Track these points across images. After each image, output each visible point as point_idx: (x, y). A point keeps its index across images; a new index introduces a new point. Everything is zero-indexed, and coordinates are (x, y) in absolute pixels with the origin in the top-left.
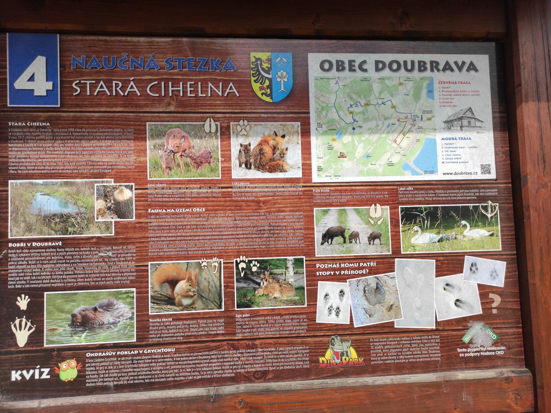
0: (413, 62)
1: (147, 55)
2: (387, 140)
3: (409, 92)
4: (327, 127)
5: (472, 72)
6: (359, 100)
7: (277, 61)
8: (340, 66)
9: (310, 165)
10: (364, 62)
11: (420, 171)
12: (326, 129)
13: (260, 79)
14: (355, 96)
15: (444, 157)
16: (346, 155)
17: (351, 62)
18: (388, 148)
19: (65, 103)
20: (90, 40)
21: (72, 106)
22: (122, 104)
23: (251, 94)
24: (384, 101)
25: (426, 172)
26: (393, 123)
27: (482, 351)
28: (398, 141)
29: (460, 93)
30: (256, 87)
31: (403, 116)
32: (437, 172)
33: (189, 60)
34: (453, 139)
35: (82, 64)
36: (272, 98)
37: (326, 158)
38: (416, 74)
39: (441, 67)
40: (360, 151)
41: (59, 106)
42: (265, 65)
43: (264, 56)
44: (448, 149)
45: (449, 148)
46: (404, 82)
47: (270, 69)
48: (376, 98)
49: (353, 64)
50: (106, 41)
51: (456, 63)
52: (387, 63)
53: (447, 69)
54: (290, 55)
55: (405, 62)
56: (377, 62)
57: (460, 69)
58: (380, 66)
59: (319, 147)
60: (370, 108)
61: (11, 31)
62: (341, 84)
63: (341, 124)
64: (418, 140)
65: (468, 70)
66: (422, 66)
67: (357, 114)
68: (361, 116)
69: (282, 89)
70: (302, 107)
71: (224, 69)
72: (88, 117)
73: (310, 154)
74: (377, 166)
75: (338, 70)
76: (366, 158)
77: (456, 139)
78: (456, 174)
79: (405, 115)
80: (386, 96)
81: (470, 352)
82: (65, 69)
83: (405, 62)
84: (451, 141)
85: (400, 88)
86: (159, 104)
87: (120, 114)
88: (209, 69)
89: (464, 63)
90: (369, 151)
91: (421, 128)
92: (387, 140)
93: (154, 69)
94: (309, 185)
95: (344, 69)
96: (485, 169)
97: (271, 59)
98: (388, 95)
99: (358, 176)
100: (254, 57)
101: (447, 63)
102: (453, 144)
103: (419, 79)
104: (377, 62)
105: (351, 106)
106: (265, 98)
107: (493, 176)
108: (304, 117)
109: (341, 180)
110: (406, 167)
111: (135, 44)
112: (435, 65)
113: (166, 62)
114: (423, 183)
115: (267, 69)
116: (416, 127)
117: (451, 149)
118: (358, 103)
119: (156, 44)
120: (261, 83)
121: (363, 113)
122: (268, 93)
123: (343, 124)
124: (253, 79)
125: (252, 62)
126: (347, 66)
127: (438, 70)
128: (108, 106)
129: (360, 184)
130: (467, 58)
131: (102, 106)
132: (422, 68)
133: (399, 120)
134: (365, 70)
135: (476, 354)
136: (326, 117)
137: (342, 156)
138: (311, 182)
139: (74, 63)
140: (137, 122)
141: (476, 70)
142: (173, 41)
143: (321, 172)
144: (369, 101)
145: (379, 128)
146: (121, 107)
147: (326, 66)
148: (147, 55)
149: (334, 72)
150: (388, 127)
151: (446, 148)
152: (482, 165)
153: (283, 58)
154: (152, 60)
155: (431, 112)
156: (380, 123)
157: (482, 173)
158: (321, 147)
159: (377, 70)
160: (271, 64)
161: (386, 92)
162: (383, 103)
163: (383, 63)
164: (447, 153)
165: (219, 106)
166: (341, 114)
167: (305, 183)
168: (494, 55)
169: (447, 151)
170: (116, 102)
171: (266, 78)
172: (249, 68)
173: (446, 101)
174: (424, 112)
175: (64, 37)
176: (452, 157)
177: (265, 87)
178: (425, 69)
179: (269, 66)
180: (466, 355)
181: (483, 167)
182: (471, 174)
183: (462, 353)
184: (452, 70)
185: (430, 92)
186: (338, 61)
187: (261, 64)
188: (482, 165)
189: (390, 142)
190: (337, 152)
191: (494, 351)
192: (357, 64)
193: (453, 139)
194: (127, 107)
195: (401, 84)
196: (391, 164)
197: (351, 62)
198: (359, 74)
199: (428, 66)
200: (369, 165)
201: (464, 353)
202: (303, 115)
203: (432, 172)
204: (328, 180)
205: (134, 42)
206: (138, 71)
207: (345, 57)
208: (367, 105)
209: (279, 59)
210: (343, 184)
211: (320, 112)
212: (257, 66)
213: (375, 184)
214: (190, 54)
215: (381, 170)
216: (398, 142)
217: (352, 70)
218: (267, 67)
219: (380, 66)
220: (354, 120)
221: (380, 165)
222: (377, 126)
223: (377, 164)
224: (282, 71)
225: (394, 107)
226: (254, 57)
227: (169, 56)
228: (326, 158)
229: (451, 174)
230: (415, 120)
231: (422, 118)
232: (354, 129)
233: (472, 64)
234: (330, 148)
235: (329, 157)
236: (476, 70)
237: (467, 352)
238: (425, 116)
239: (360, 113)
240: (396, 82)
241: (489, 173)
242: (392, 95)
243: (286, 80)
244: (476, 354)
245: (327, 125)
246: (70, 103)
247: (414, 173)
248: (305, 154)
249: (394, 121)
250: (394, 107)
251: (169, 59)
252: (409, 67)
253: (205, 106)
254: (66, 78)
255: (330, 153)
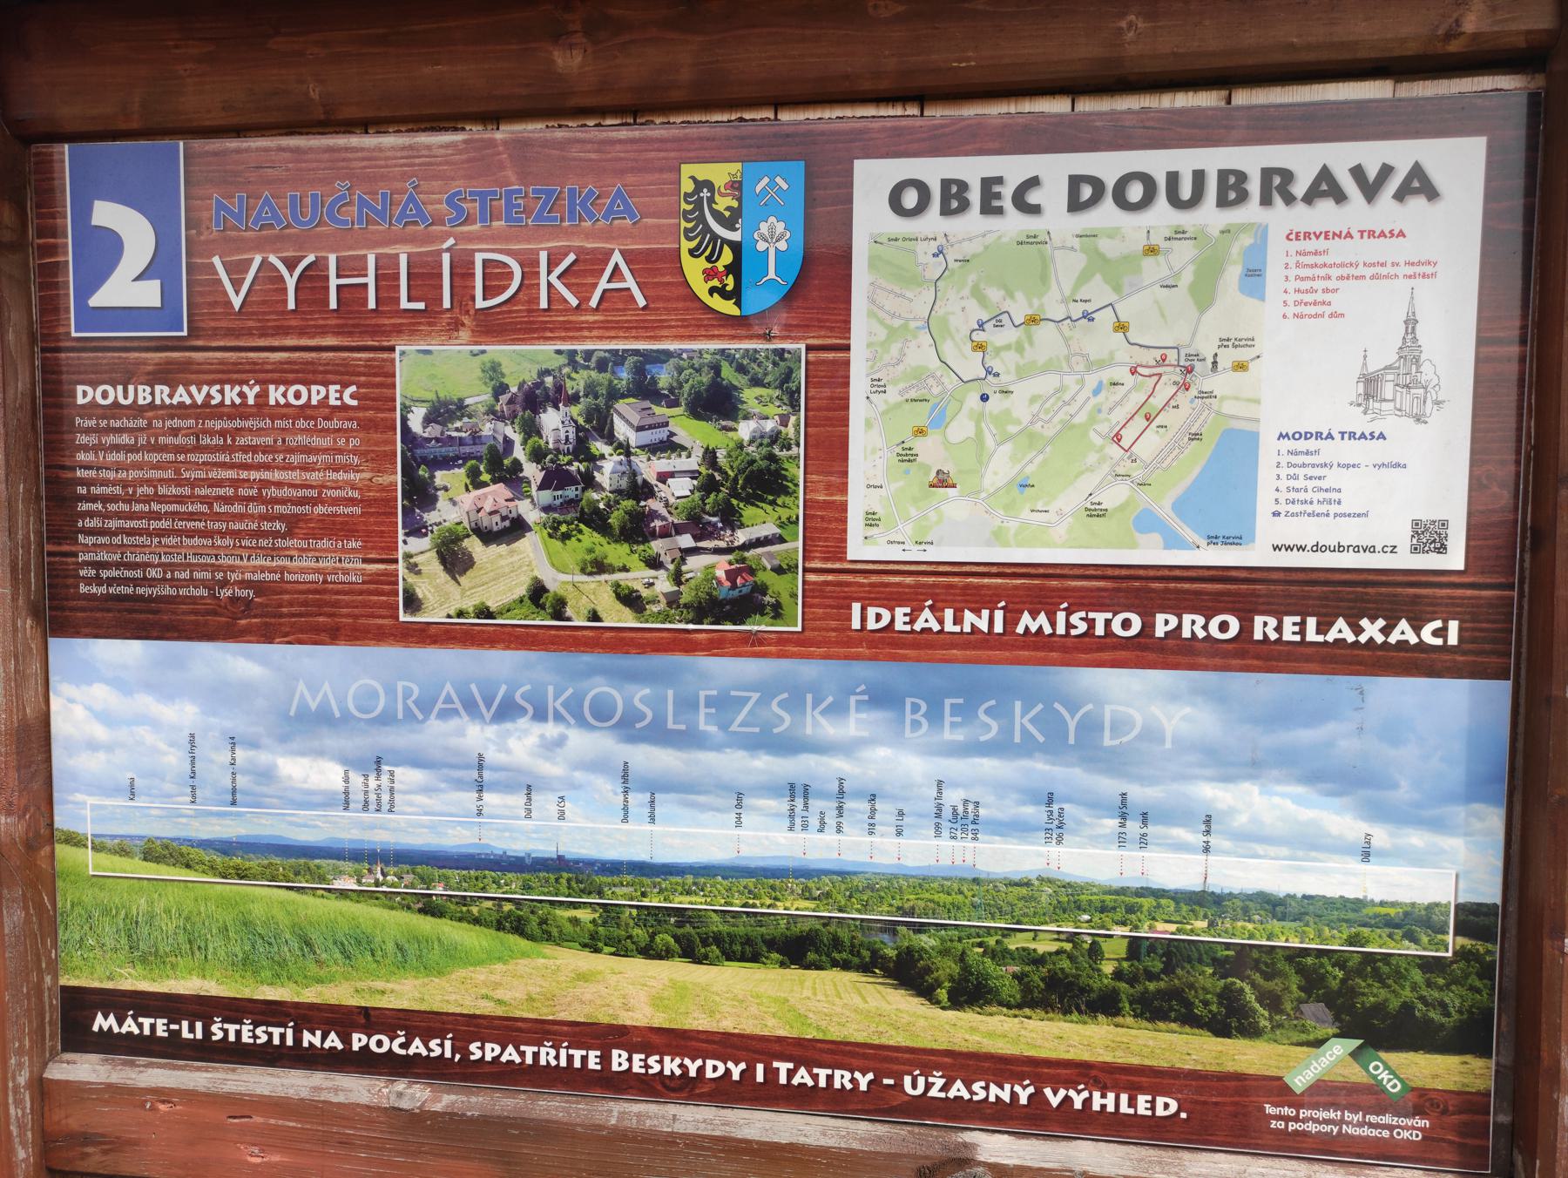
0: (1199, 177)
1: (398, 185)
2: (1092, 434)
3: (1177, 275)
4: (901, 393)
5: (1417, 203)
6: (1008, 305)
7: (758, 189)
8: (954, 198)
9: (843, 507)
10: (1034, 182)
11: (1189, 534)
12: (899, 399)
13: (709, 247)
14: (994, 294)
15: (1282, 497)
16: (954, 478)
17: (990, 185)
18: (1092, 458)
19: (202, 325)
20: (258, 149)
21: (215, 332)
22: (338, 326)
23: (682, 291)
24: (1090, 307)
25: (1213, 540)
26: (1116, 379)
27: (1348, 1123)
28: (1128, 437)
29: (1369, 272)
30: (694, 269)
31: (1150, 357)
32: (1253, 540)
33: (509, 193)
34: (1319, 435)
35: (238, 217)
36: (738, 304)
37: (894, 486)
38: (1209, 215)
39: (1299, 189)
40: (1001, 468)
41: (185, 333)
42: (723, 203)
43: (719, 173)
44: (1297, 471)
45: (1304, 465)
46: (1164, 245)
47: (736, 213)
48: (1064, 301)
49: (996, 189)
50: (297, 150)
51: (1358, 173)
52: (1110, 184)
53: (1324, 194)
54: (799, 167)
55: (1173, 178)
56: (1075, 182)
57: (1370, 190)
58: (1086, 192)
59: (874, 451)
60: (1044, 332)
61: (72, 138)
62: (950, 259)
63: (946, 380)
64: (1196, 437)
65: (1400, 196)
66: (1233, 187)
67: (998, 350)
68: (1011, 357)
69: (772, 275)
70: (831, 329)
71: (605, 217)
72: (255, 364)
73: (845, 474)
74: (1052, 517)
75: (946, 211)
76: (1016, 491)
77: (1330, 436)
78: (1317, 548)
79: (1158, 354)
80: (1098, 292)
81: (1304, 1121)
82: (200, 233)
83: (1173, 178)
84: (1312, 444)
85: (1148, 262)
86: (430, 324)
87: (331, 354)
88: (562, 220)
89: (1386, 171)
90: (1029, 469)
91: (1210, 395)
92: (1092, 434)
93: (416, 223)
94: (837, 566)
95: (964, 206)
96: (1429, 536)
97: (740, 183)
98: (1107, 288)
99: (989, 544)
100: (693, 178)
101: (1325, 174)
102: (1317, 452)
103: (1216, 233)
104: (1075, 182)
105: (981, 326)
106: (717, 303)
107: (1455, 559)
108: (834, 362)
109: (933, 554)
110: (1147, 522)
111: (371, 155)
112: (1277, 184)
113: (449, 202)
114: (1201, 573)
115: (727, 214)
116: (1193, 392)
117: (1310, 472)
118: (1005, 318)
119: (424, 152)
120: (708, 259)
121: (1019, 348)
122: (729, 288)
123: (950, 381)
124: (686, 245)
125: (686, 195)
126: (975, 196)
127: (1289, 199)
128: (302, 332)
129: (994, 570)
130: (1401, 154)
131: (287, 334)
132: (1232, 195)
133: (1133, 372)
134: (1035, 210)
135: (1328, 1128)
136: (899, 361)
137: (942, 481)
138: (843, 559)
139: (218, 214)
140: (375, 375)
141: (1432, 193)
142: (465, 142)
143: (874, 531)
144: (1042, 306)
145: (1067, 397)
146: (337, 334)
147: (910, 199)
148: (398, 185)
149: (933, 219)
150: (1096, 392)
151: (1290, 465)
152: (1416, 523)
153: (778, 180)
154: (411, 199)
155: (1249, 342)
156: (1070, 380)
157: (1415, 550)
158: (880, 453)
159: (1075, 205)
160: (740, 200)
161: (1098, 277)
162: (1087, 316)
163: (1098, 185)
164: (1292, 483)
165: (590, 329)
166: (948, 349)
167: (826, 559)
168: (1515, 134)
169: (1295, 477)
170: (321, 322)
171: (724, 241)
172: (676, 213)
173: (1309, 298)
174: (1224, 342)
175: (198, 144)
176: (1308, 496)
177: (721, 269)
178: (1243, 197)
179: (735, 204)
180: (1292, 1126)
181: (1418, 528)
182: (1371, 549)
183: (1279, 1118)
184: (1340, 197)
185: (1254, 274)
186: (946, 184)
187: (711, 200)
188: (1416, 523)
189: (1098, 441)
190: (929, 468)
191: (1391, 1128)
192: (1007, 191)
193: (1319, 435)
194: (350, 334)
195: (1152, 251)
196: (1096, 512)
197: (989, 184)
198: (1014, 223)
199: (1254, 187)
200: (1026, 514)
201: (1287, 1119)
202: (830, 355)
203: (1233, 541)
204: (895, 554)
205: (368, 150)
206: (378, 231)
207: (971, 169)
208: (1033, 320)
209: (766, 180)
210: (941, 569)
211: (882, 344)
212: (699, 205)
213: (1041, 571)
214: (513, 178)
215: (1062, 530)
216: (1125, 443)
217: (990, 207)
218: (728, 209)
219: (1086, 192)
220: (989, 372)
221: (1060, 513)
222: (1061, 389)
223: (1052, 508)
224: (772, 219)
225: (1121, 327)
226: (693, 178)
227: (457, 186)
228: (894, 486)
229: (1302, 548)
230: (1189, 370)
231: (1215, 363)
232: (984, 398)
233: (1417, 171)
234: (908, 456)
235: (901, 483)
236: (1432, 193)
237: (1296, 1119)
238: (1227, 358)
239: (1008, 347)
240: (1141, 241)
241: (1442, 549)
242: (1117, 288)
243: (782, 246)
244: (1328, 1128)
245: (902, 385)
246: (213, 324)
247: (1173, 541)
248: (830, 473)
249: (1122, 374)
250: (1121, 327)
251: (459, 193)
252: (1186, 192)
253: (551, 330)
254: (201, 256)
255: (907, 472)
